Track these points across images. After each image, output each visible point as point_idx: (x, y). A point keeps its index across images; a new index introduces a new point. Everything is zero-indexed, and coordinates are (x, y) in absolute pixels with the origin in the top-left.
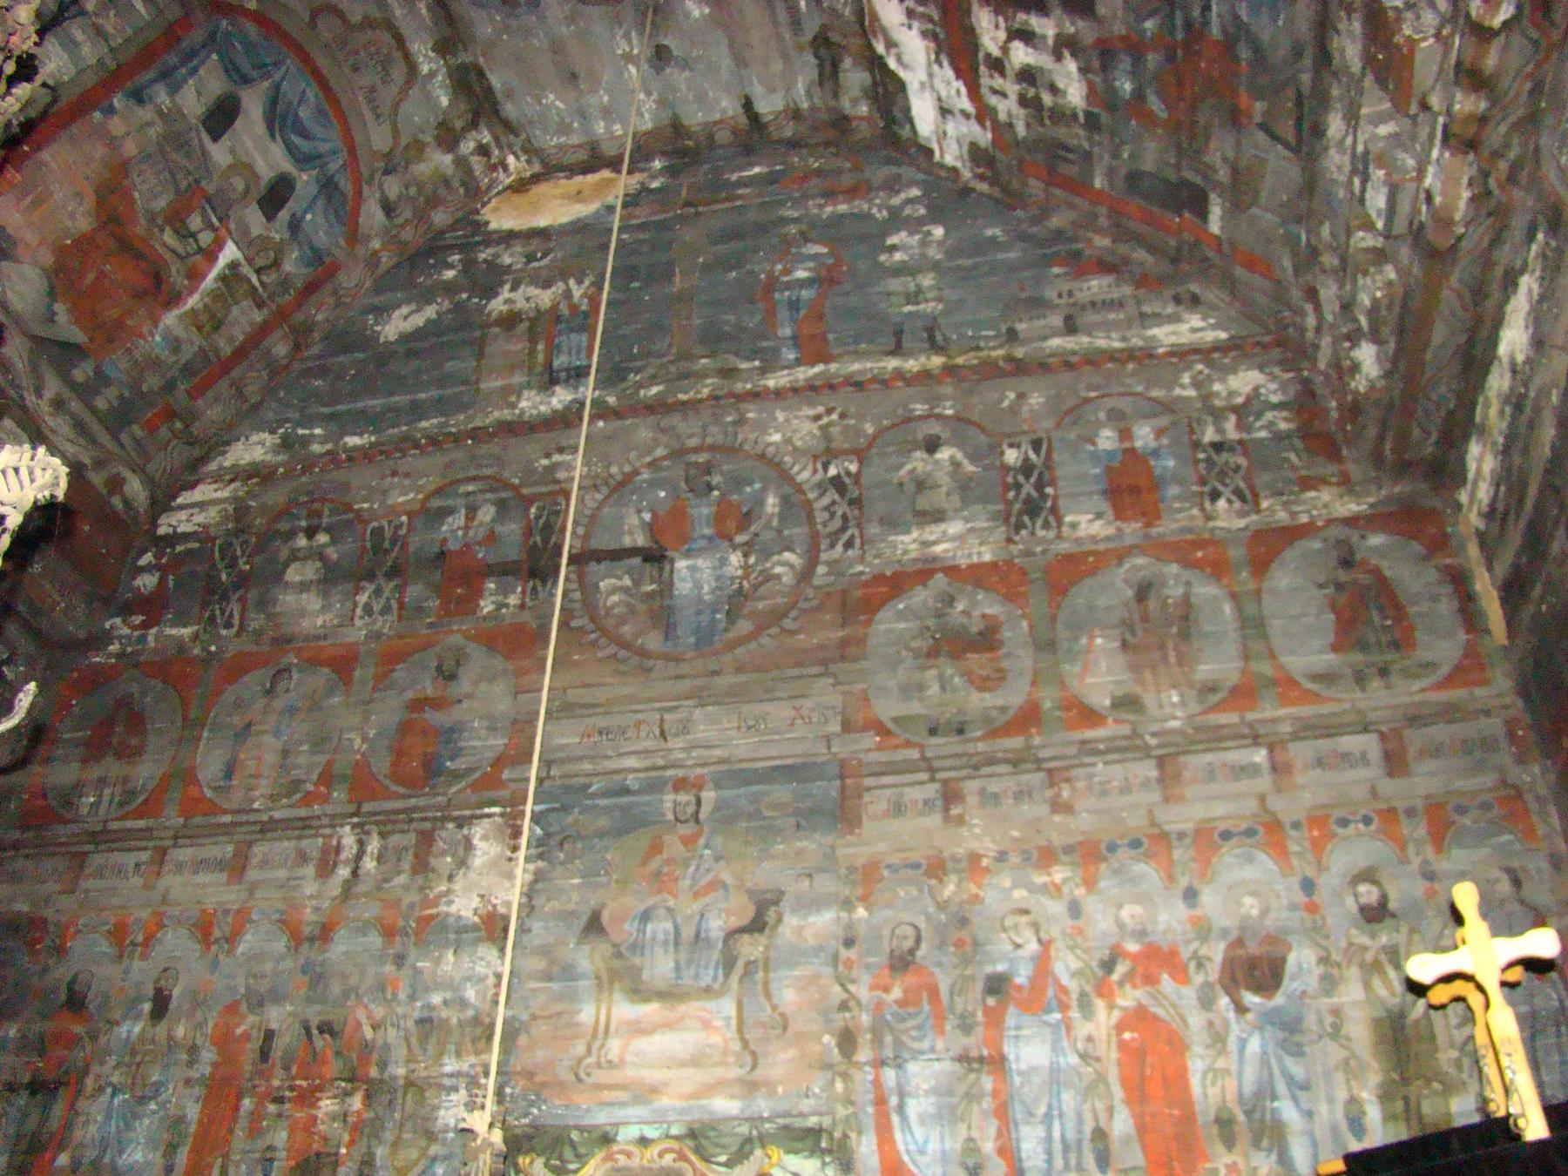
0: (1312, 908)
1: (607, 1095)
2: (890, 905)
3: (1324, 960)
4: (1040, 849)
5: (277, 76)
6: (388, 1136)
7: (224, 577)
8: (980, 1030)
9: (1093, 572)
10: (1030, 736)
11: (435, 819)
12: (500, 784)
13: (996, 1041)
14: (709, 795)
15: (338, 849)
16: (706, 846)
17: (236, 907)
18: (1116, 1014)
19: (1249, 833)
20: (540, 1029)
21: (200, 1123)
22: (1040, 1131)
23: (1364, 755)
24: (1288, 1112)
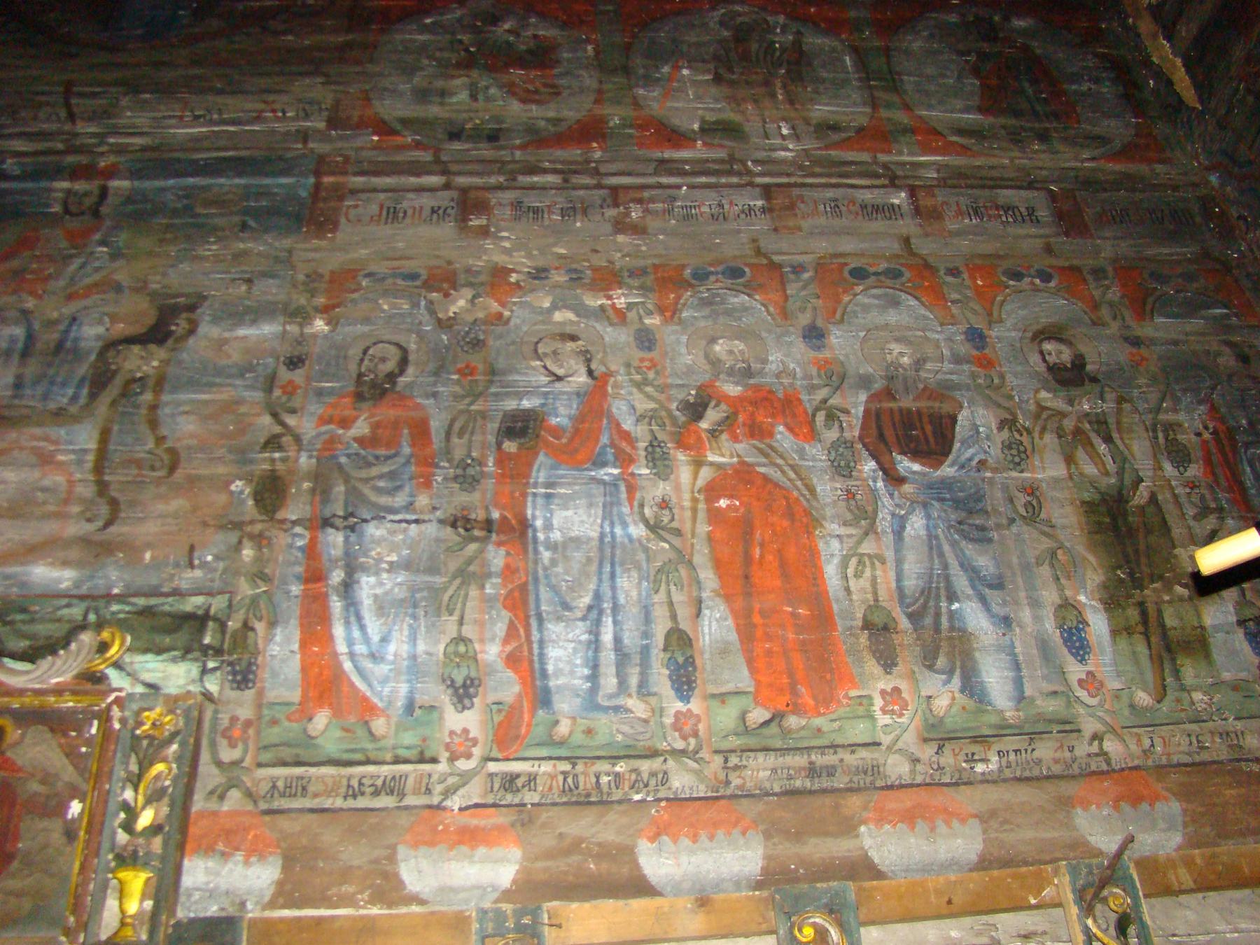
0: (986, 363)
2: (366, 320)
3: (1008, 423)
4: (595, 270)
8: (490, 484)
16: (103, 243)
18: (706, 474)
22: (580, 632)
23: (1031, 211)
24: (975, 618)
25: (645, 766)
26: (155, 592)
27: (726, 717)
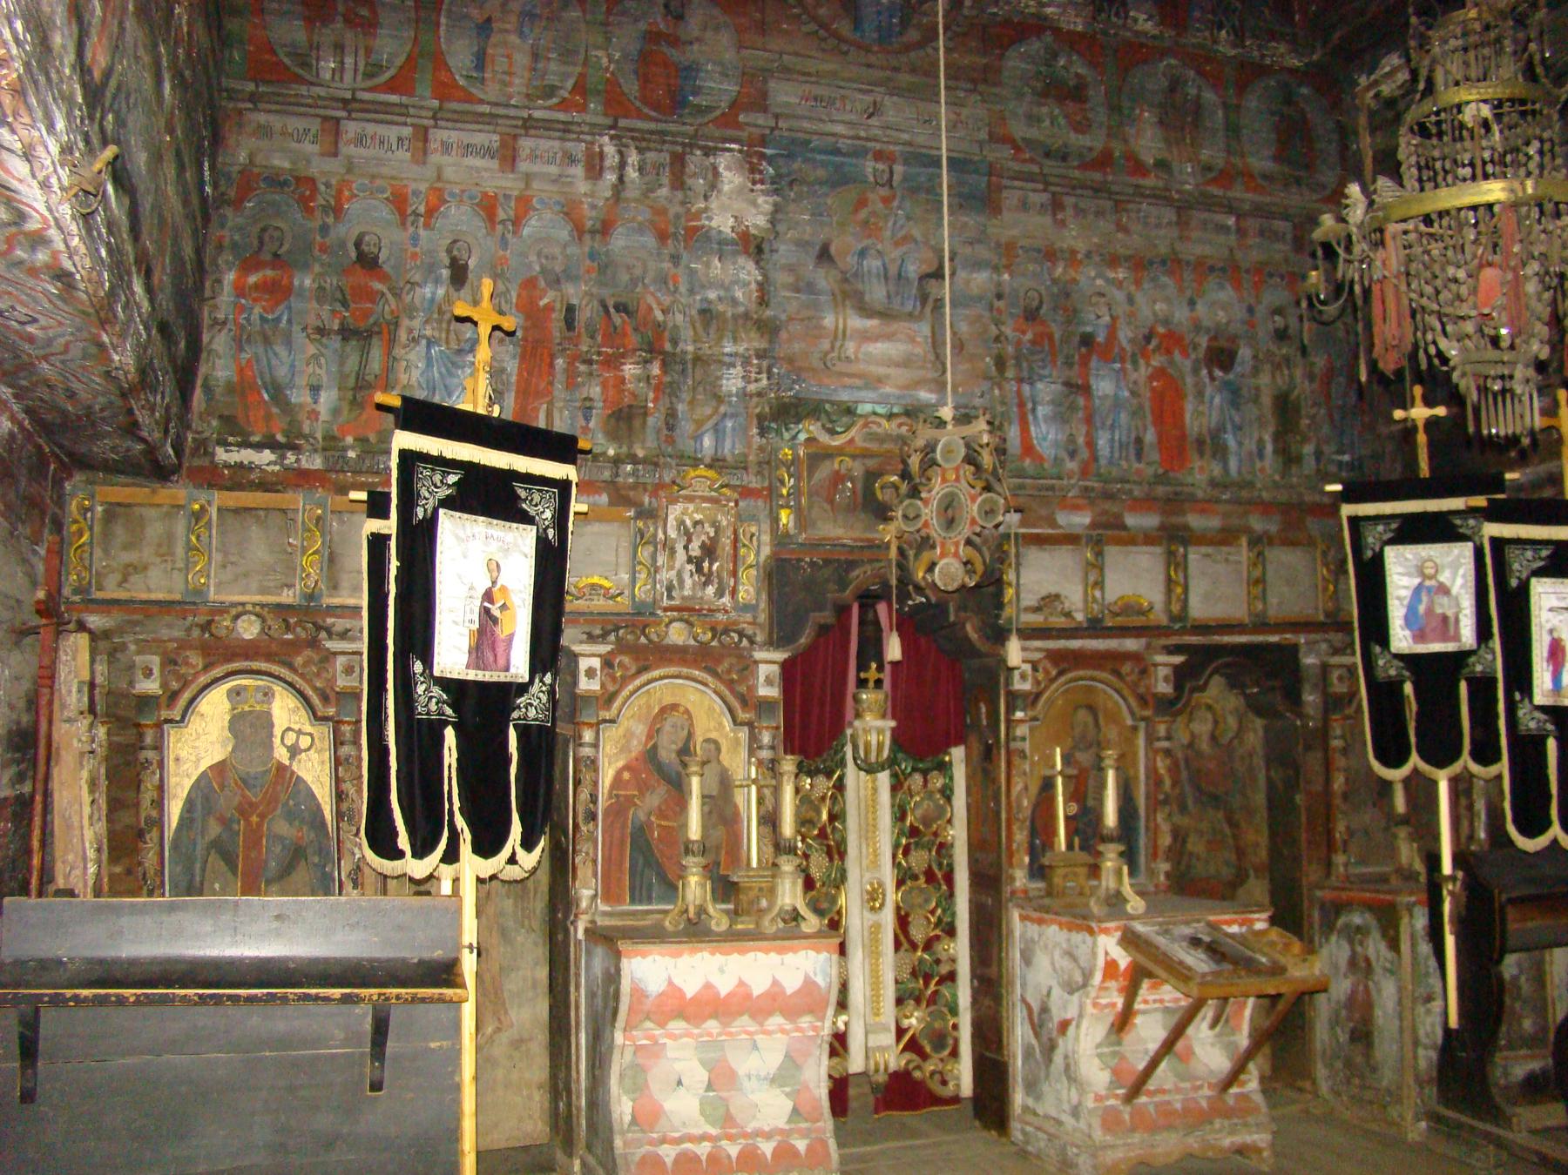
1: (847, 381)
3: (1255, 357)
6: (686, 396)
9: (1145, 61)
10: (1105, 174)
11: (684, 145)
12: (739, 126)
13: (1086, 376)
14: (899, 169)
15: (602, 155)
16: (899, 208)
17: (516, 193)
19: (1223, 270)
20: (796, 328)
21: (520, 374)
25: (1127, 486)
26: (966, 407)
27: (1150, 471)
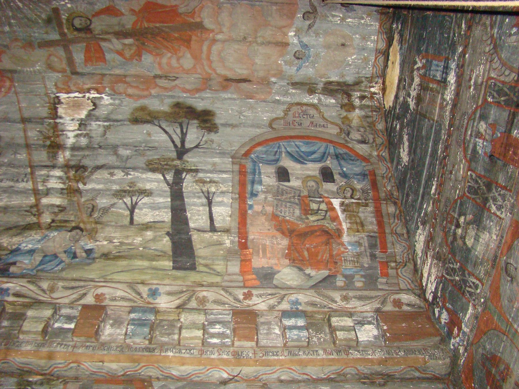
5: (283, 150)
7: (457, 278)
